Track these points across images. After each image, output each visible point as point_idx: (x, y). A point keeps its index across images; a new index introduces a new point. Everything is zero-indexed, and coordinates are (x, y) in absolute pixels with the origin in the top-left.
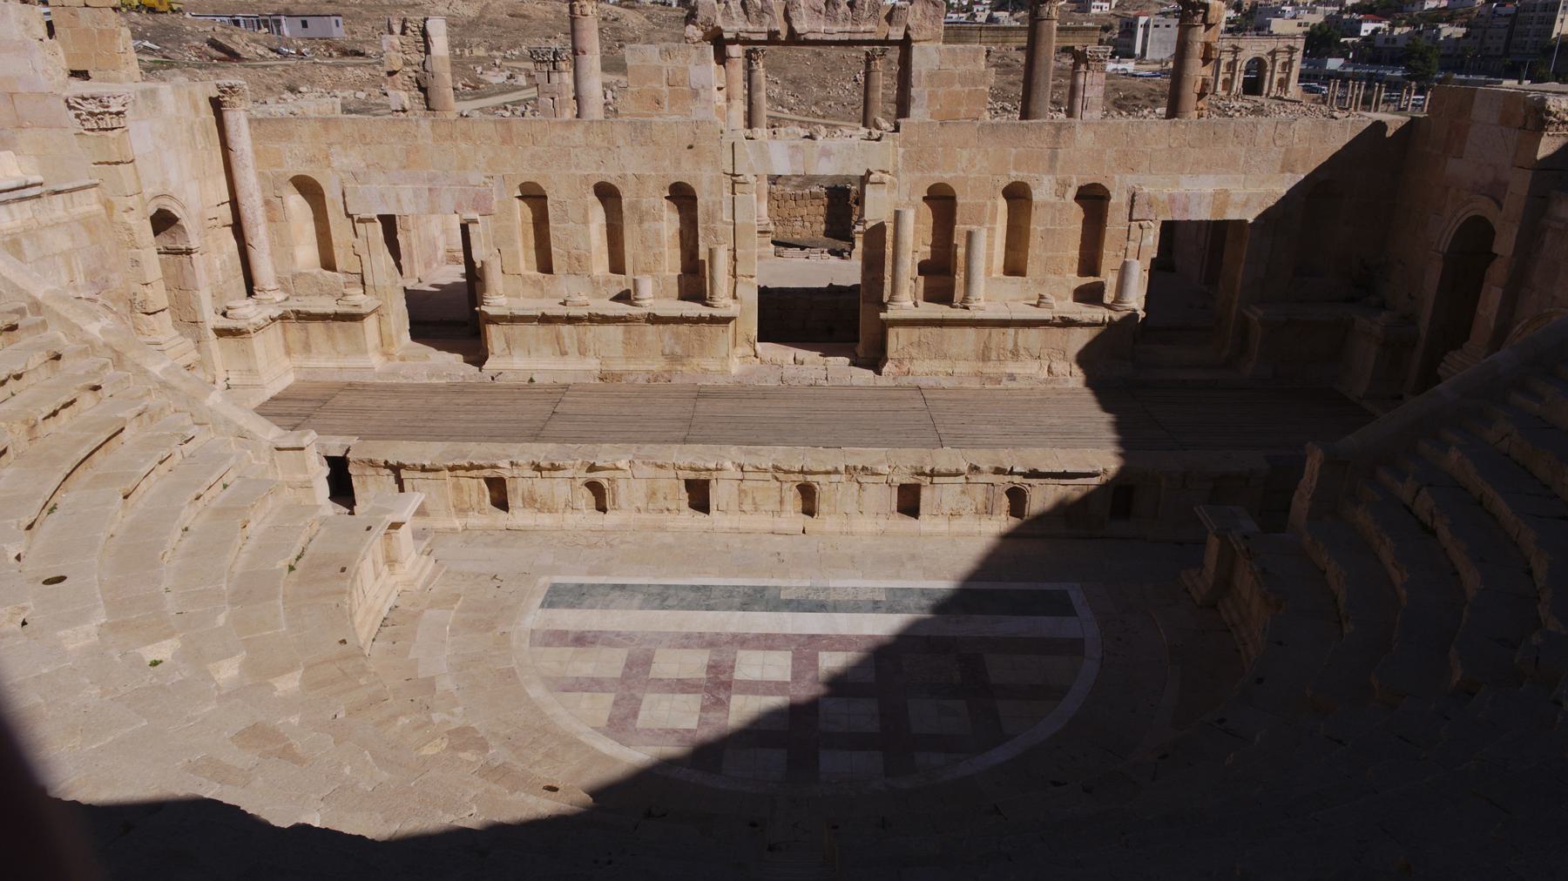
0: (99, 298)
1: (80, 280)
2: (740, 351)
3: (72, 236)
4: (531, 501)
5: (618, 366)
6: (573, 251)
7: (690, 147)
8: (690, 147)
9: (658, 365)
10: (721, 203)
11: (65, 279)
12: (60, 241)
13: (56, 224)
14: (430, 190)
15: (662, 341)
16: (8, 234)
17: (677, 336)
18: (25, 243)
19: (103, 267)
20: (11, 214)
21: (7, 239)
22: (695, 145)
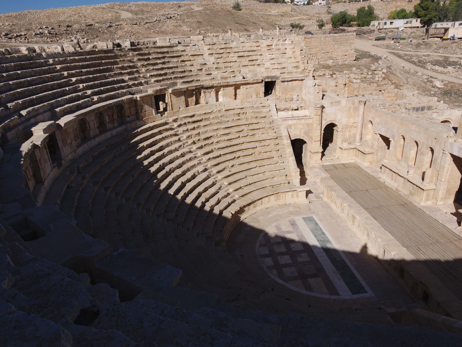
1: (302, 133)
2: (433, 201)
3: (303, 126)
4: (335, 203)
5: (400, 189)
6: (407, 156)
7: (436, 139)
8: (436, 139)
9: (407, 192)
10: (439, 157)
11: (299, 132)
13: (300, 124)
14: (387, 131)
15: (410, 187)
17: (413, 188)
18: (292, 126)
19: (309, 132)
20: (292, 121)
22: (437, 138)
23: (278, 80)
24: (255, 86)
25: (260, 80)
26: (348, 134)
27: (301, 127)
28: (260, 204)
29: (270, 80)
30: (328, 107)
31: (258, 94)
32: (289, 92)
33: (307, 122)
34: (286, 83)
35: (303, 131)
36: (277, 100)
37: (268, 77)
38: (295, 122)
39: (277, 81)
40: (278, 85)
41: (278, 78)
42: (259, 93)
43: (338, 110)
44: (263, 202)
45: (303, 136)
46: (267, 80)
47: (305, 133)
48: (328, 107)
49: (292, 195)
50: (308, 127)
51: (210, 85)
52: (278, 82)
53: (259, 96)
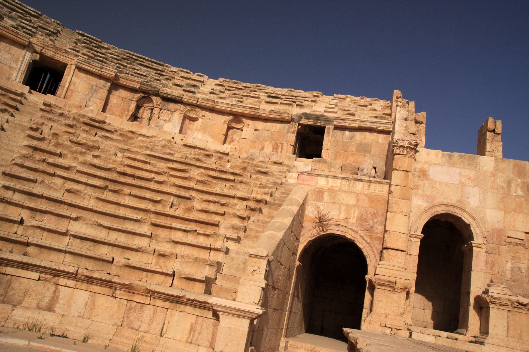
0: (360, 232)
1: (353, 220)
11: (342, 216)
12: (351, 200)
16: (318, 188)
20: (328, 182)
21: (317, 189)
23: (329, 124)
24: (276, 129)
25: (286, 115)
26: (509, 266)
27: (351, 200)
28: (45, 302)
29: (311, 122)
30: (439, 164)
31: (278, 146)
32: (353, 154)
33: (371, 191)
34: (347, 133)
35: (356, 215)
36: (317, 164)
37: (306, 116)
38: (335, 185)
39: (327, 127)
40: (328, 136)
41: (329, 121)
42: (282, 144)
43: (469, 179)
44: (61, 301)
45: (354, 228)
46: (304, 122)
47: (362, 220)
48: (439, 164)
49: (192, 329)
50: (371, 207)
51: (175, 94)
52: (329, 129)
53: (279, 150)
